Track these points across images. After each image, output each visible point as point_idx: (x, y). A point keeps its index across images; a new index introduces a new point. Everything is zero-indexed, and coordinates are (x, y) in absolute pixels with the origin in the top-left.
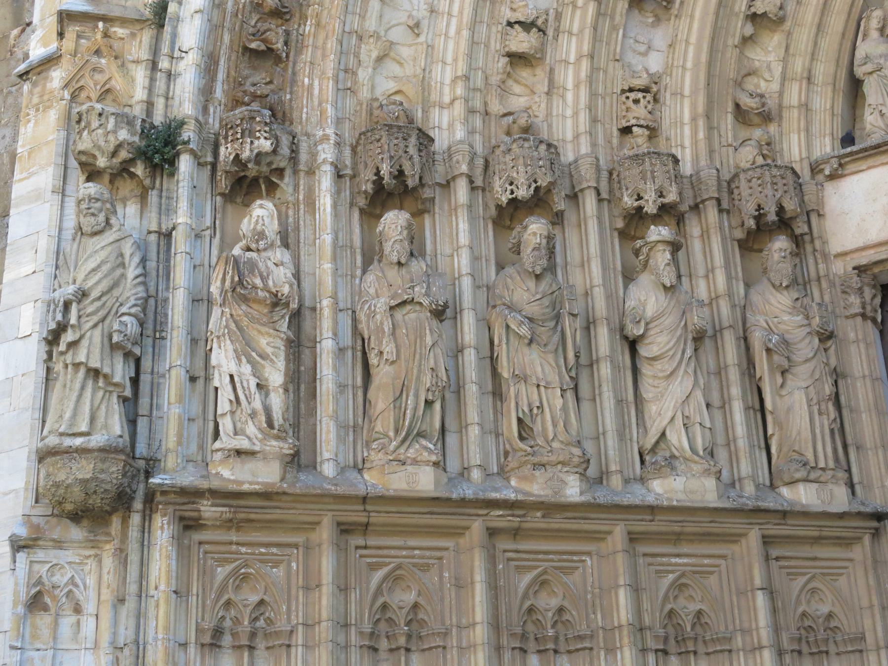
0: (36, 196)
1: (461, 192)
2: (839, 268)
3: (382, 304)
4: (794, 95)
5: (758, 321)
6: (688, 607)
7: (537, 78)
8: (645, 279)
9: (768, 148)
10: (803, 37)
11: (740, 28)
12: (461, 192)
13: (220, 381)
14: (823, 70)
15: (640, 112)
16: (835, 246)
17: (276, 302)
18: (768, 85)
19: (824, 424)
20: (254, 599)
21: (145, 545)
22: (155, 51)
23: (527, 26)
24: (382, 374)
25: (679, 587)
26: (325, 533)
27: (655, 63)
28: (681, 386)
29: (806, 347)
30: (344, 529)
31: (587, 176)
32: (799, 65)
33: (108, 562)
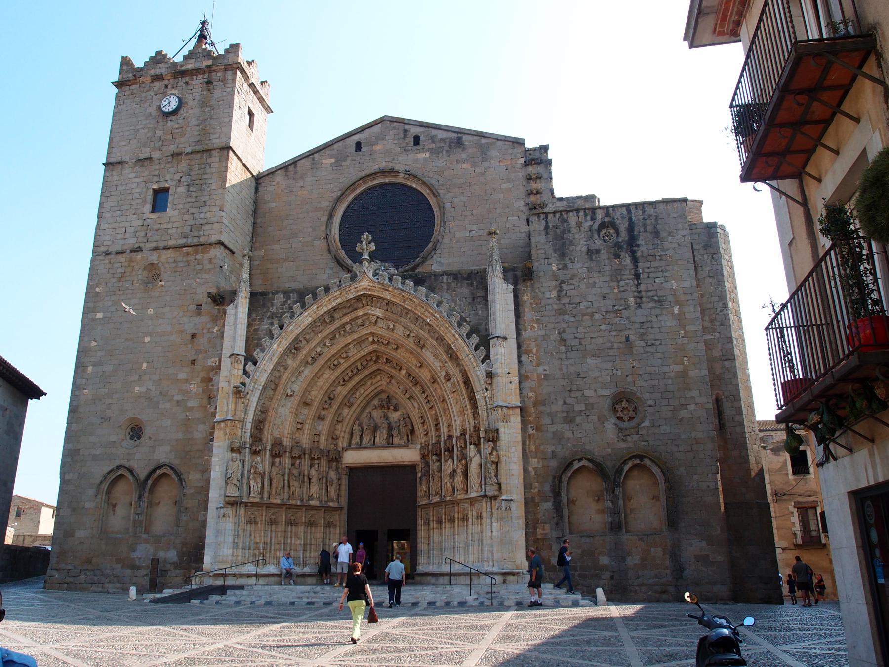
0: (219, 446)
1: (288, 454)
2: (344, 466)
3: (275, 473)
4: (342, 435)
5: (329, 476)
6: (312, 519)
7: (301, 432)
8: (313, 469)
9: (336, 445)
10: (345, 424)
11: (335, 422)
12: (288, 454)
13: (252, 486)
14: (347, 430)
15: (316, 439)
16: (344, 462)
17: (260, 474)
18: (338, 433)
19: (336, 494)
20: (253, 517)
21: (240, 509)
22: (242, 427)
23: (301, 424)
24: (274, 485)
25: (312, 516)
26: (264, 508)
27: (320, 428)
28: (316, 487)
29: (336, 481)
30: (267, 507)
31: (307, 451)
32: (344, 429)
33: (234, 511)
